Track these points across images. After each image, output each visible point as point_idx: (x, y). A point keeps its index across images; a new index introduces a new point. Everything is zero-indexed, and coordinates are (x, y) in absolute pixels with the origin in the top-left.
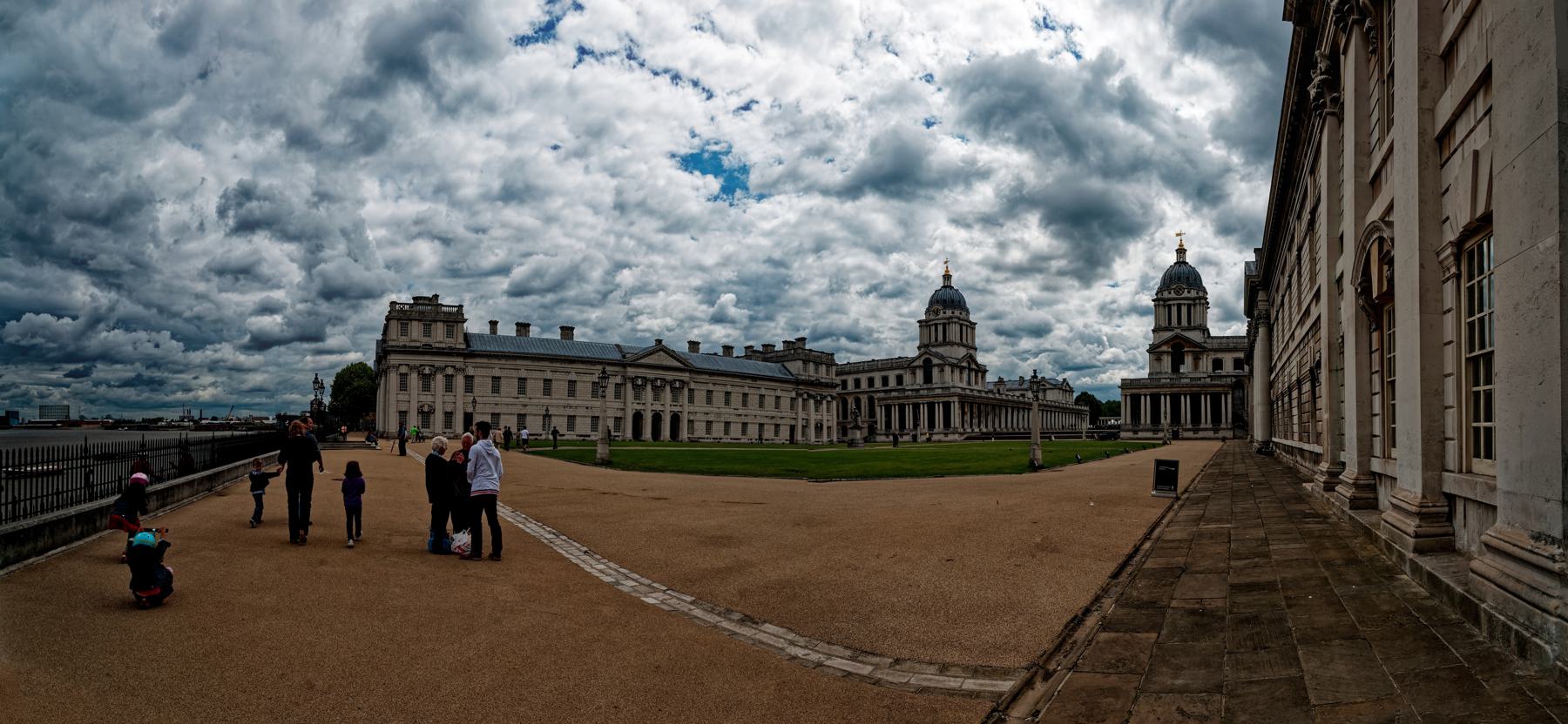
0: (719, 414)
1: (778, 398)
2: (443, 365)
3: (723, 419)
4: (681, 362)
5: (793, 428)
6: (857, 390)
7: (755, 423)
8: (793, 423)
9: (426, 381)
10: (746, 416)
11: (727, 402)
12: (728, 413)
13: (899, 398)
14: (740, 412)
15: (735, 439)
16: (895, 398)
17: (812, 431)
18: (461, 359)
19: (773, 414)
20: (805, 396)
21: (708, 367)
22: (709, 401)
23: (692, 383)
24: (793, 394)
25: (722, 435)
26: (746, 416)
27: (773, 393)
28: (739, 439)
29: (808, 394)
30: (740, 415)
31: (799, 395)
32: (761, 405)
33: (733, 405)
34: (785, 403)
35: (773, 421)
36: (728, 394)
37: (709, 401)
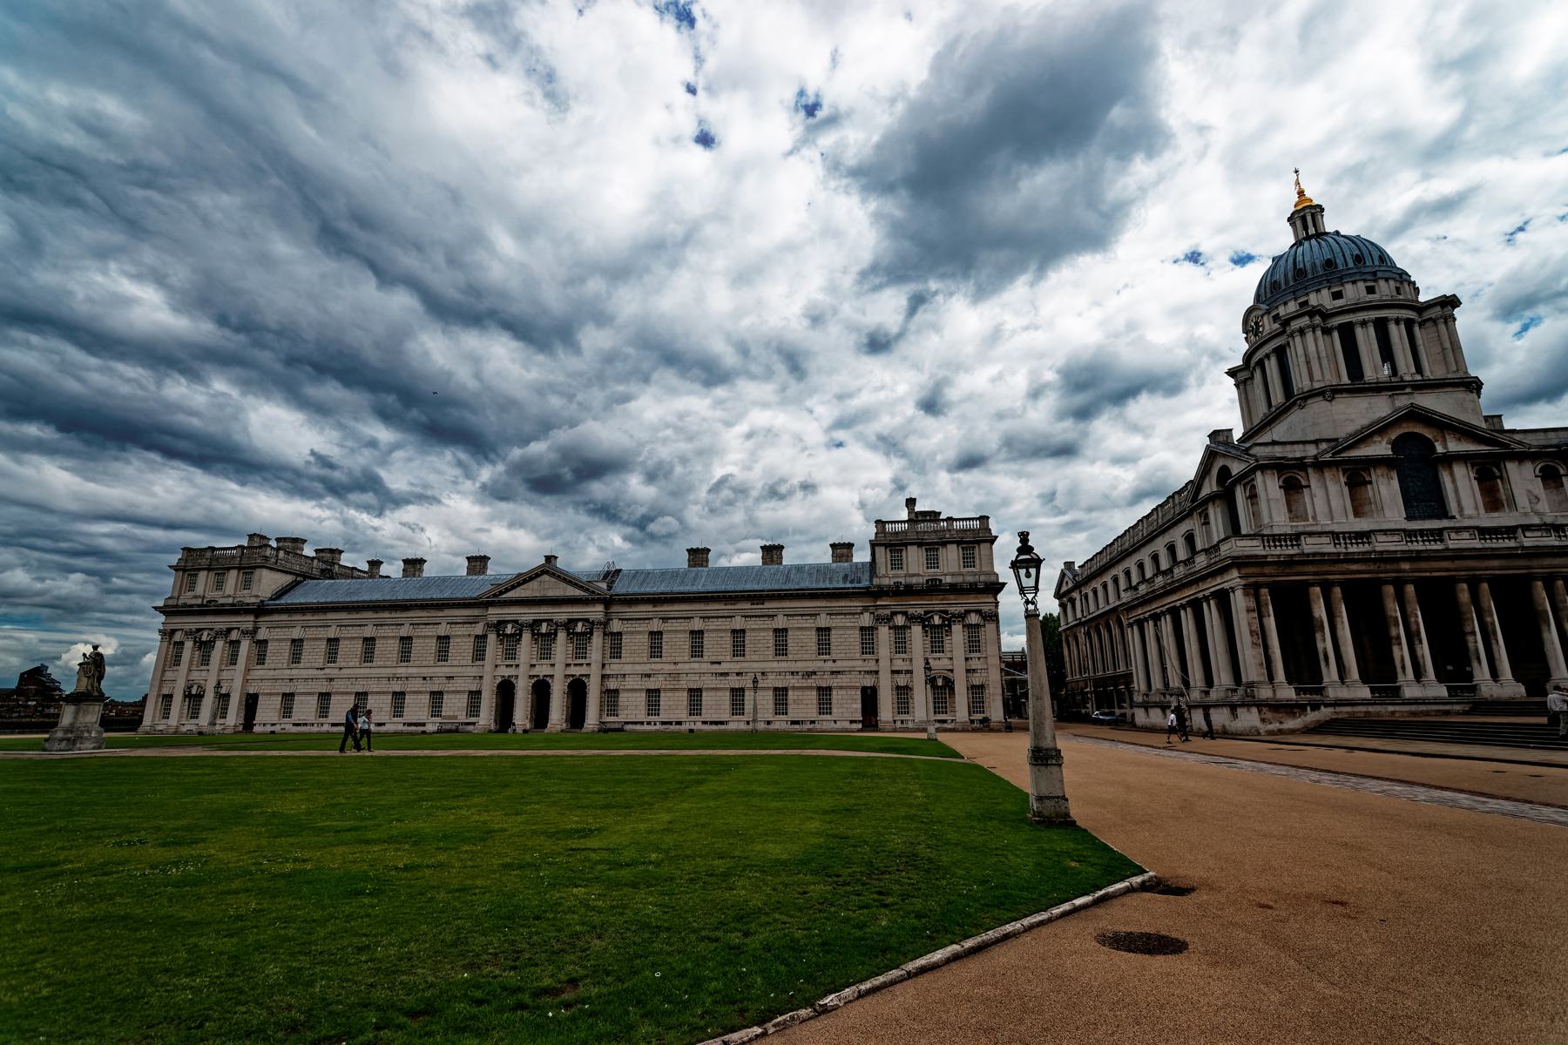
0: (675, 676)
1: (823, 632)
2: (224, 627)
3: (685, 683)
4: (581, 588)
5: (869, 698)
7: (810, 688)
8: (868, 681)
9: (205, 647)
10: (738, 674)
11: (697, 650)
12: (697, 672)
14: (724, 668)
15: (712, 723)
17: (921, 698)
18: (251, 618)
19: (811, 666)
20: (900, 620)
21: (668, 589)
22: (656, 650)
23: (615, 621)
24: (866, 619)
25: (683, 714)
26: (738, 674)
27: (809, 623)
28: (722, 723)
30: (727, 674)
32: (781, 649)
33: (708, 655)
34: (846, 639)
35: (811, 682)
36: (697, 635)
37: (656, 650)
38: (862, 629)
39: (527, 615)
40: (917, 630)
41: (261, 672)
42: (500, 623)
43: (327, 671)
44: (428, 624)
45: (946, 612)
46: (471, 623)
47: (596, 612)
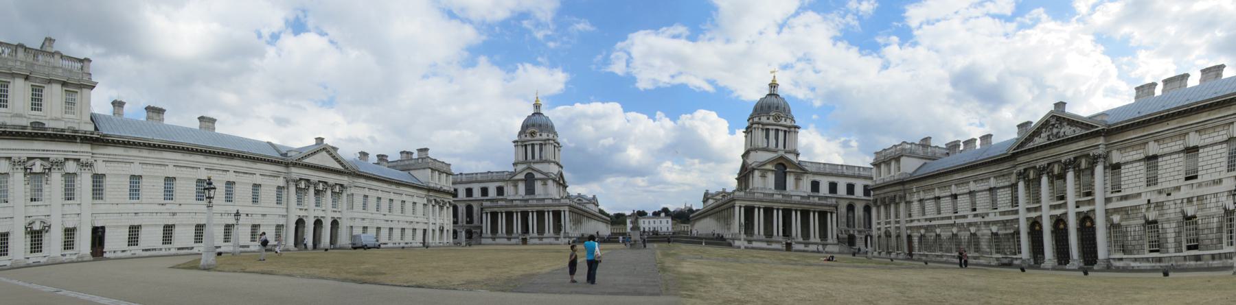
6: (468, 199)
13: (507, 207)
16: (502, 206)
20: (433, 202)
29: (435, 200)
31: (429, 201)
38: (424, 204)
39: (315, 176)
40: (437, 206)
41: (103, 207)
42: (301, 179)
43: (167, 206)
44: (246, 173)
45: (443, 201)
46: (274, 176)
47: (344, 180)
